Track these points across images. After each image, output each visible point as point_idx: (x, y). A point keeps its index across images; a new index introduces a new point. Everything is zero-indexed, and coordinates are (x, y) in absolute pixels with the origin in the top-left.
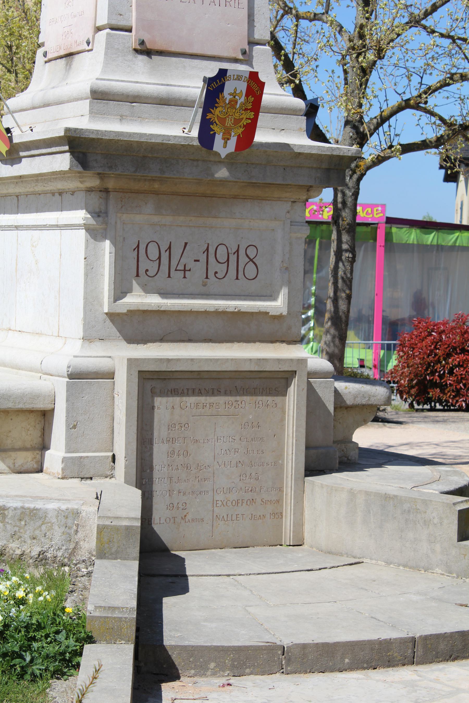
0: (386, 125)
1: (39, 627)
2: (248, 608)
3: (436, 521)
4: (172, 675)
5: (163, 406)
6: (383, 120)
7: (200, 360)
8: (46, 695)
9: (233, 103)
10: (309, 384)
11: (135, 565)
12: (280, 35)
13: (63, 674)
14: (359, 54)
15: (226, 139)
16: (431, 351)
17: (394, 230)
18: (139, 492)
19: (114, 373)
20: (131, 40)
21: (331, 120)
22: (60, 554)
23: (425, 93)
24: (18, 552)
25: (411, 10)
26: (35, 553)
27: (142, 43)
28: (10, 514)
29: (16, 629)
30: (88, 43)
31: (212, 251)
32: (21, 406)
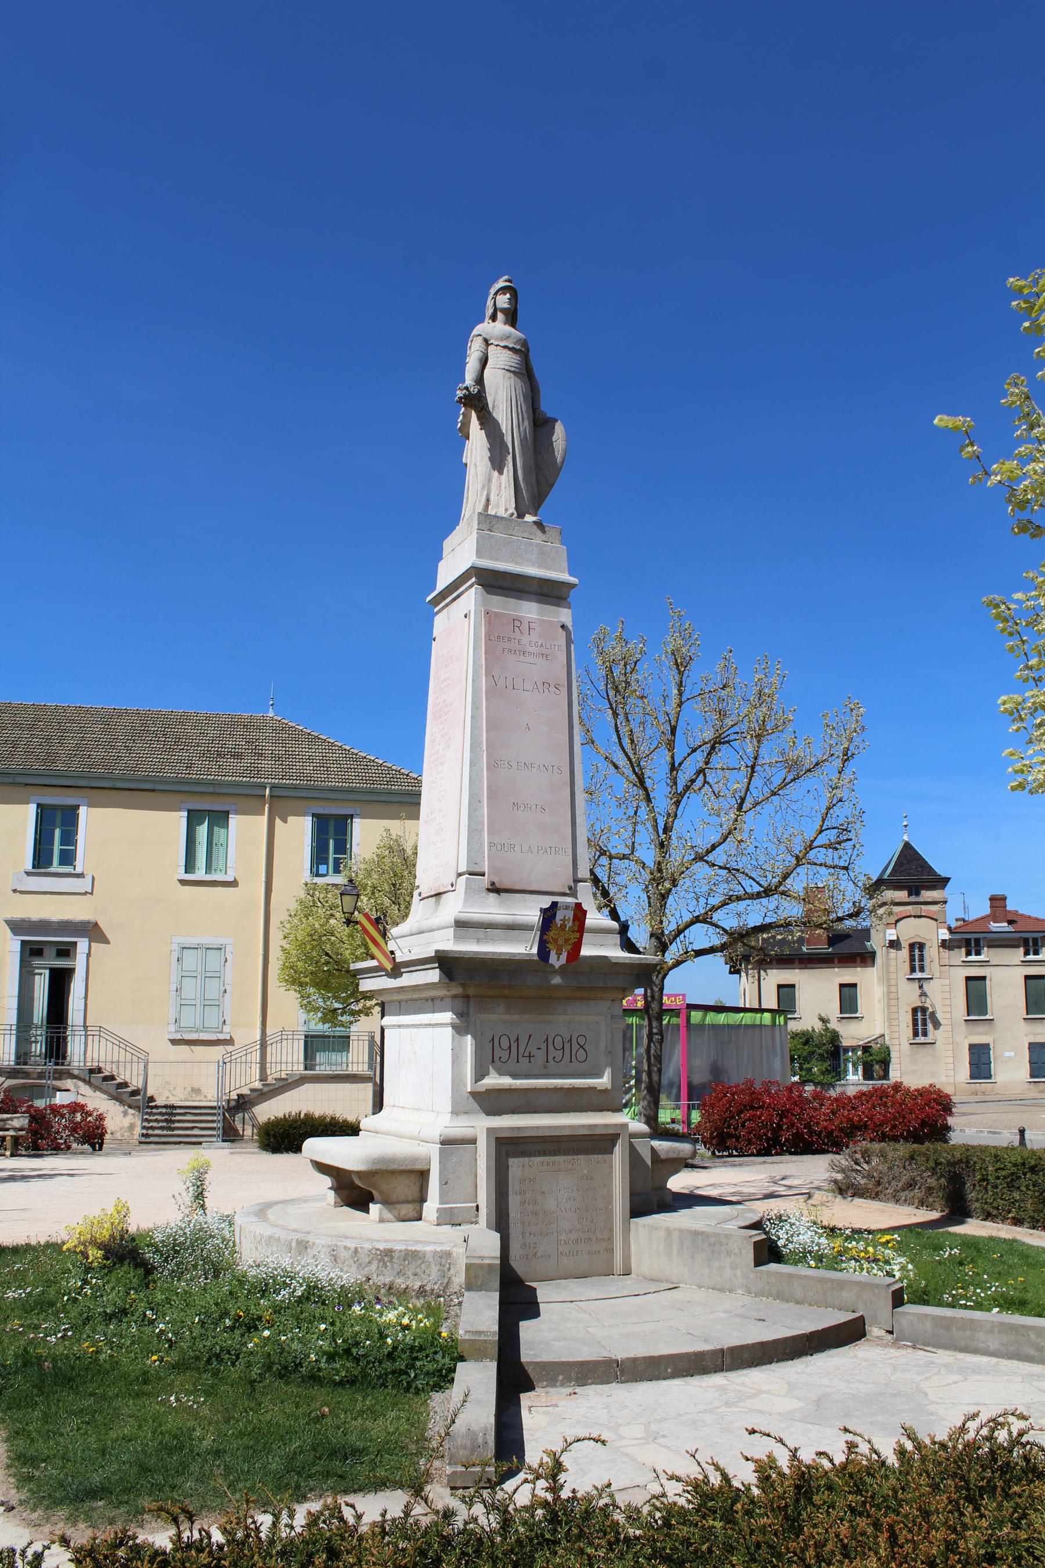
0: (682, 936)
1: (421, 1349)
2: (589, 1329)
3: (736, 1251)
4: (530, 1387)
5: (516, 1166)
6: (680, 932)
7: (543, 1128)
8: (428, 1405)
9: (563, 926)
10: (631, 1143)
11: (497, 1295)
12: (598, 871)
13: (441, 1387)
14: (658, 884)
15: (559, 954)
16: (727, 1109)
17: (693, 1013)
18: (497, 1236)
19: (476, 1140)
20: (485, 882)
21: (640, 935)
22: (436, 1287)
23: (710, 910)
24: (403, 1286)
25: (696, 849)
26: (416, 1287)
27: (493, 884)
28: (396, 1255)
29: (402, 1350)
30: (452, 885)
31: (550, 1040)
32: (403, 1167)
